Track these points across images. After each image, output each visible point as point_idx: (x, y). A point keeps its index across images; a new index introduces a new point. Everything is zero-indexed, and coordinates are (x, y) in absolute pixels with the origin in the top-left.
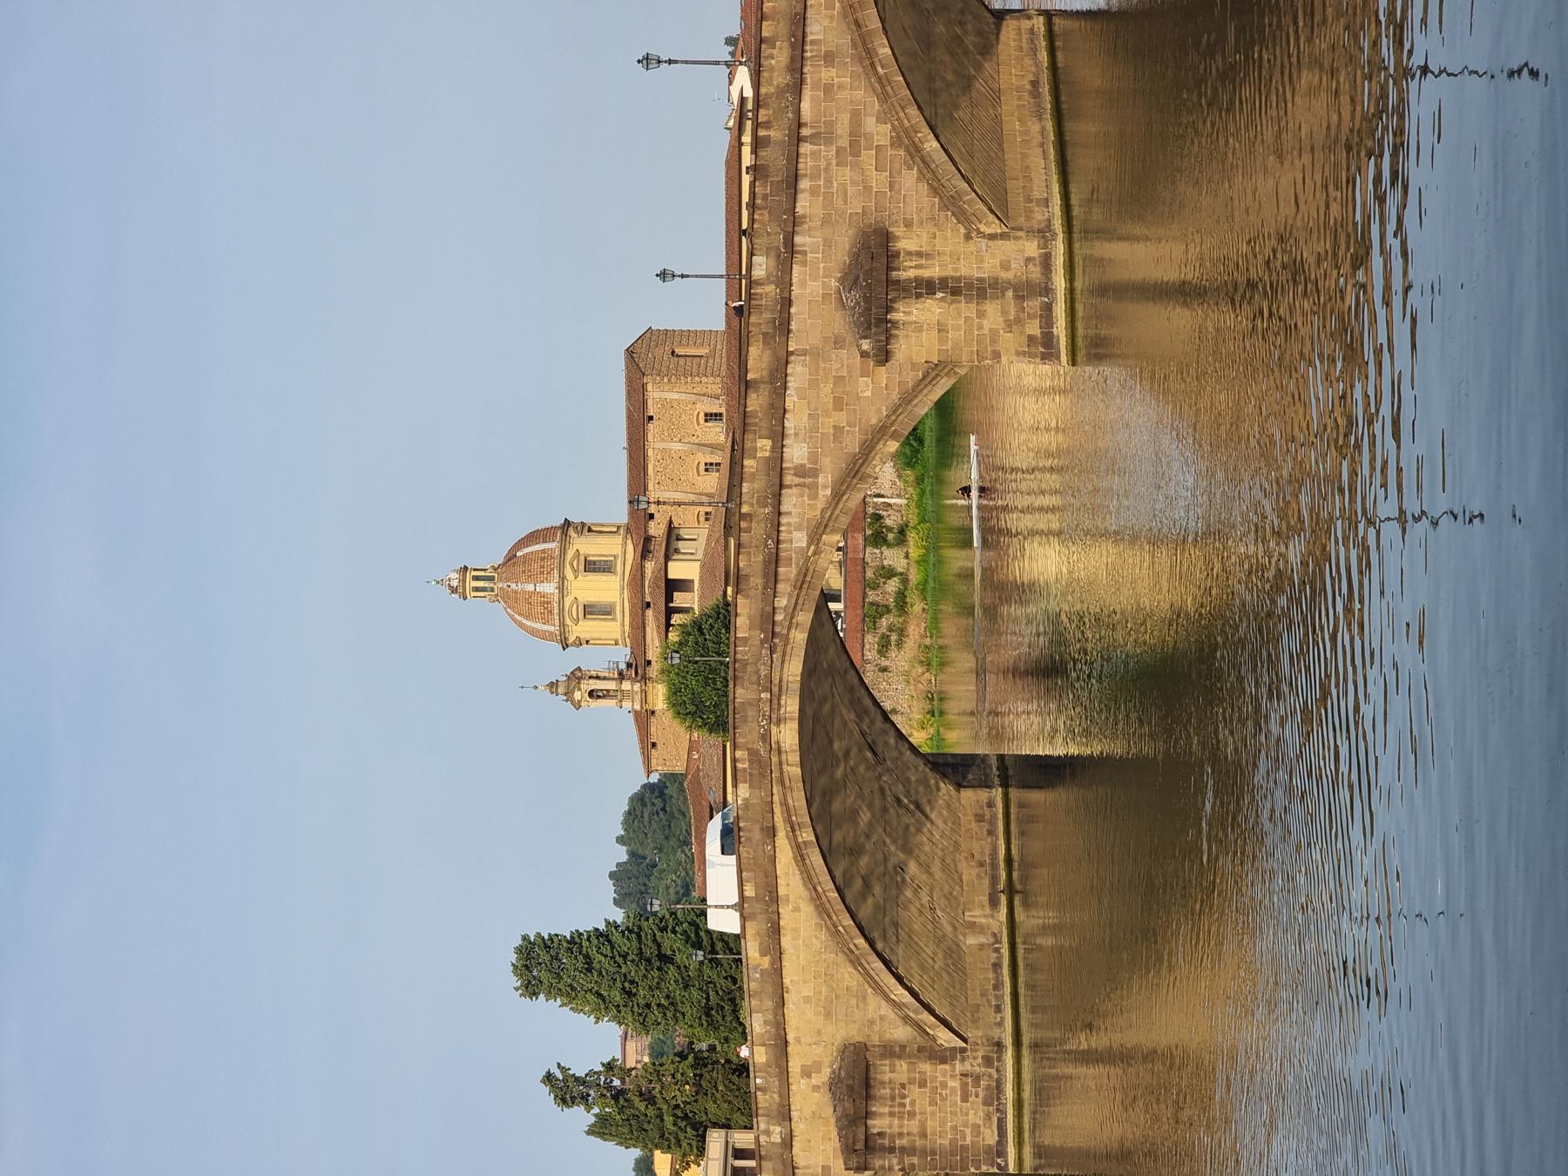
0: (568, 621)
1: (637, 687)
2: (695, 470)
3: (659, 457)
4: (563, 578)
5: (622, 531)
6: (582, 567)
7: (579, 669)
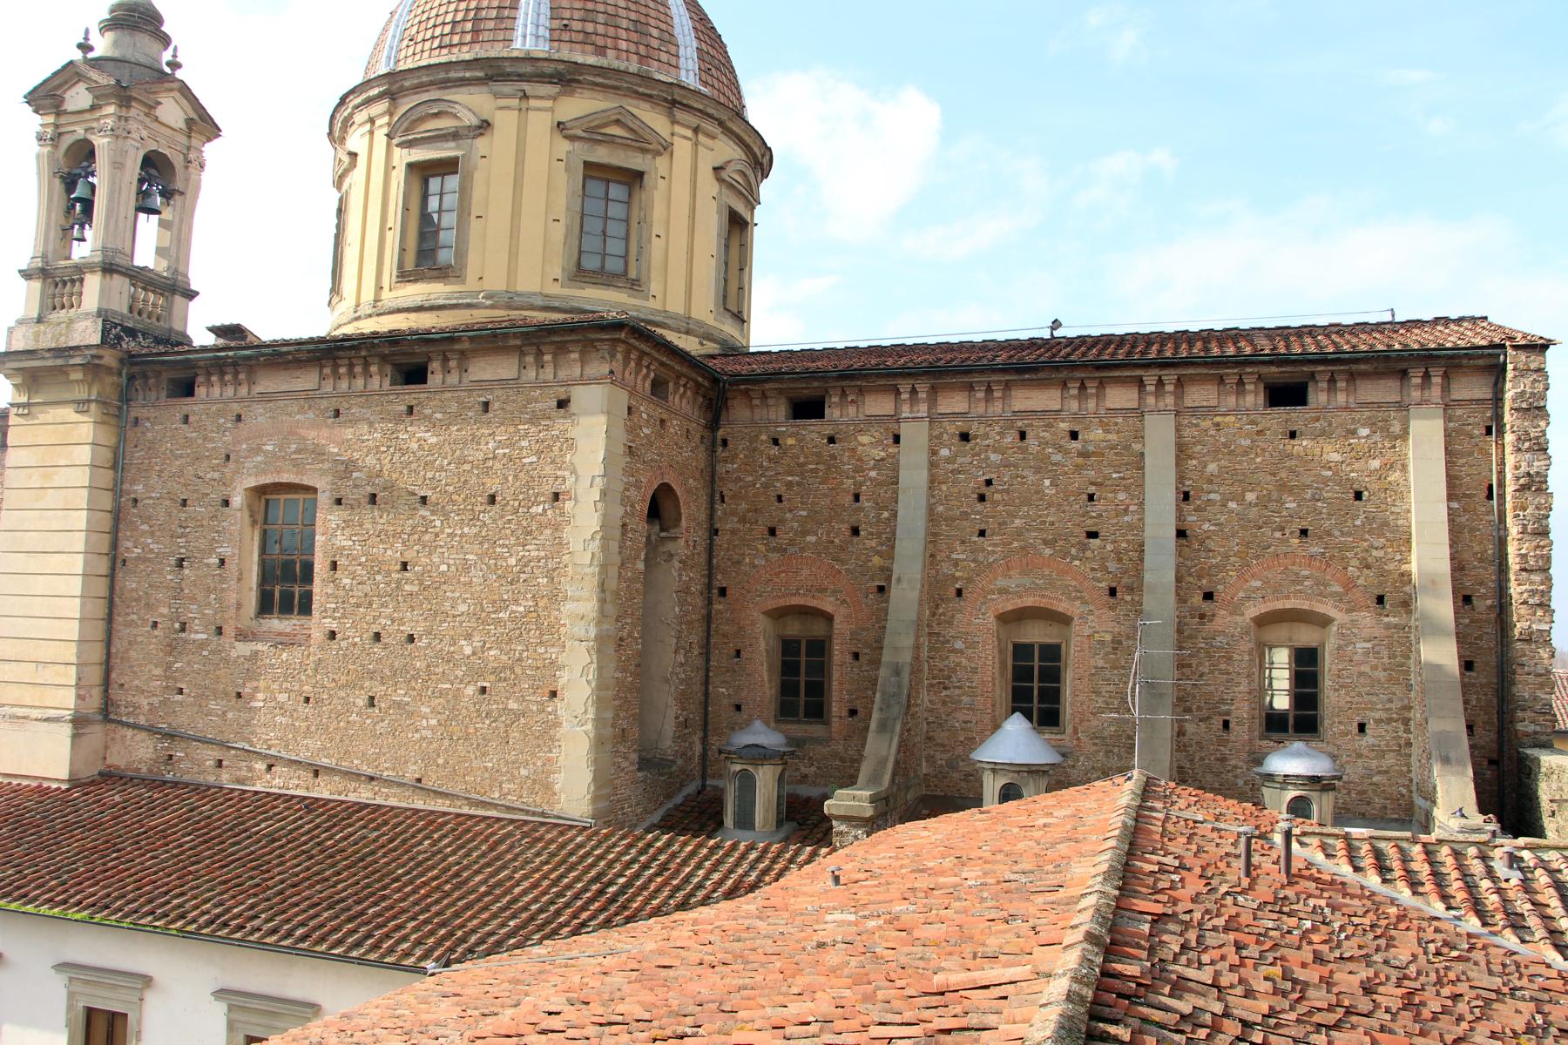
0: (405, 105)
1: (87, 333)
2: (1029, 601)
3: (1097, 434)
4: (566, 78)
5: (729, 328)
6: (602, 155)
7: (203, 125)
